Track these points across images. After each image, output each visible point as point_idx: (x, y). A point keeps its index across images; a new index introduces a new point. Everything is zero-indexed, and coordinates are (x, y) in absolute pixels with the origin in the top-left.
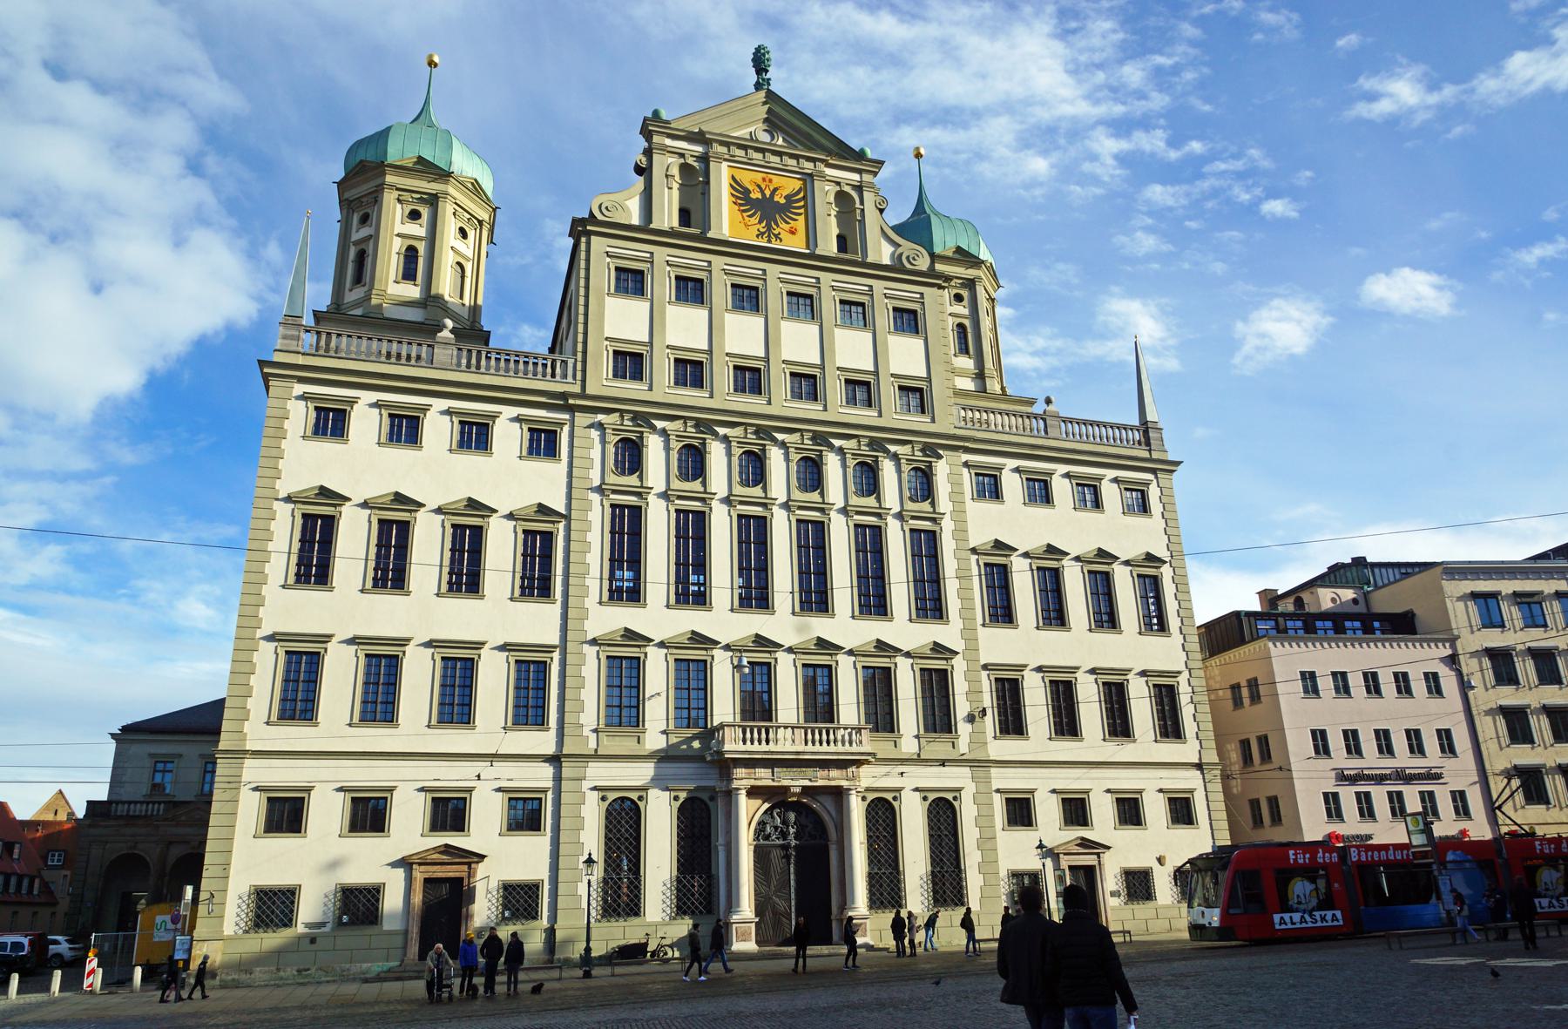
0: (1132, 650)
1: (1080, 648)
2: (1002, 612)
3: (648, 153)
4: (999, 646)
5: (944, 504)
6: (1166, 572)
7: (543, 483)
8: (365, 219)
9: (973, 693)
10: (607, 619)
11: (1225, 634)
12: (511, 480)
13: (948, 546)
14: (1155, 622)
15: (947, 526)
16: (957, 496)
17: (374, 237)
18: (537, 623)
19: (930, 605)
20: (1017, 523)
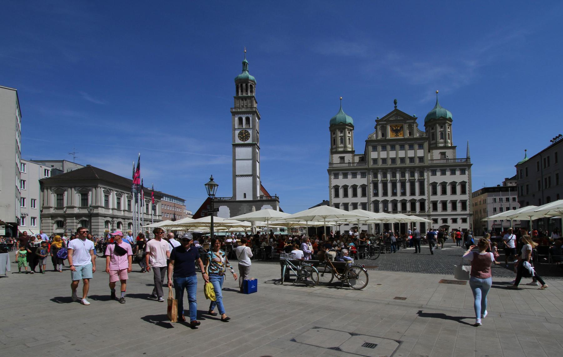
0: (459, 197)
1: (449, 197)
2: (435, 193)
3: (377, 125)
4: (433, 198)
5: (426, 177)
6: (467, 184)
7: (364, 181)
8: (334, 134)
9: (429, 205)
10: (373, 199)
11: (475, 195)
12: (360, 181)
13: (426, 183)
14: (463, 192)
15: (426, 180)
16: (428, 176)
17: (336, 137)
18: (365, 200)
19: (422, 193)
20: (439, 178)
